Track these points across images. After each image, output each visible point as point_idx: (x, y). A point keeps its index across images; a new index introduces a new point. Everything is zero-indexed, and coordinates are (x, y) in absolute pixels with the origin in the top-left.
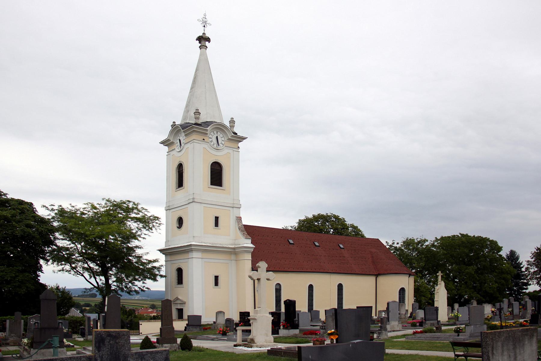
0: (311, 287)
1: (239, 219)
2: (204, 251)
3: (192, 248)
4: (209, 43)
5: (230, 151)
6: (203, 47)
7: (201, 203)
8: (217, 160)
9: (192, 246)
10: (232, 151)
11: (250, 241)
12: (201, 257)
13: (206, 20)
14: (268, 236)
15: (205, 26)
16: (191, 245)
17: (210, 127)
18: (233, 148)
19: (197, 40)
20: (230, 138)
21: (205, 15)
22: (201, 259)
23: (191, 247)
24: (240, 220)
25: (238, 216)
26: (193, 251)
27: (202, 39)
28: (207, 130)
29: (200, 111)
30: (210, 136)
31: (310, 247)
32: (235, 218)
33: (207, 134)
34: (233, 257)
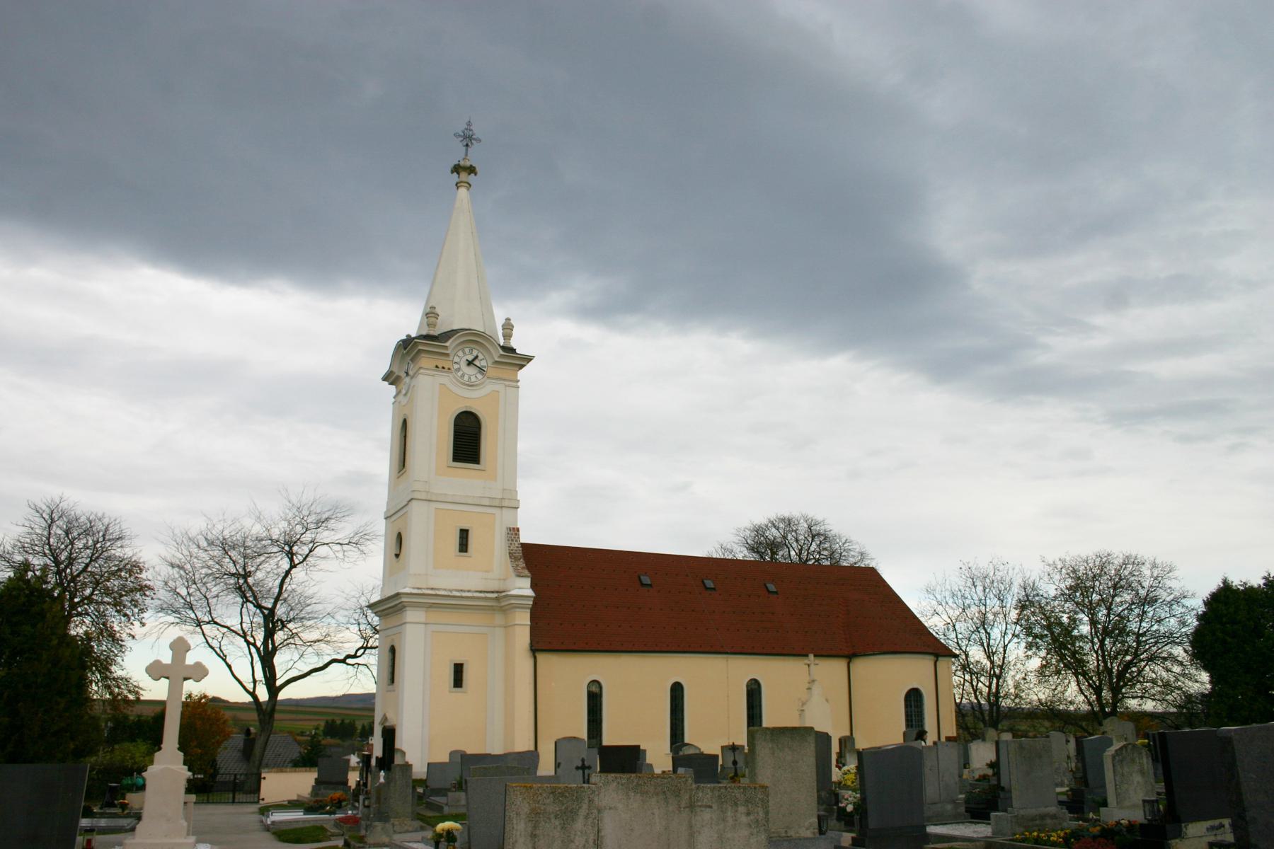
0: (677, 692)
1: (515, 531)
2: (430, 607)
3: (403, 600)
4: (476, 174)
5: (499, 387)
6: (462, 184)
7: (429, 501)
8: (470, 407)
9: (402, 596)
10: (503, 386)
11: (527, 582)
12: (423, 620)
13: (471, 133)
14: (592, 569)
15: (469, 144)
16: (398, 595)
17: (455, 339)
18: (504, 380)
19: (452, 172)
20: (498, 360)
21: (469, 124)
22: (423, 626)
23: (401, 598)
24: (516, 534)
25: (511, 527)
26: (407, 608)
27: (460, 170)
28: (447, 347)
29: (438, 311)
30: (456, 359)
31: (690, 593)
32: (504, 531)
33: (447, 355)
34: (499, 619)
